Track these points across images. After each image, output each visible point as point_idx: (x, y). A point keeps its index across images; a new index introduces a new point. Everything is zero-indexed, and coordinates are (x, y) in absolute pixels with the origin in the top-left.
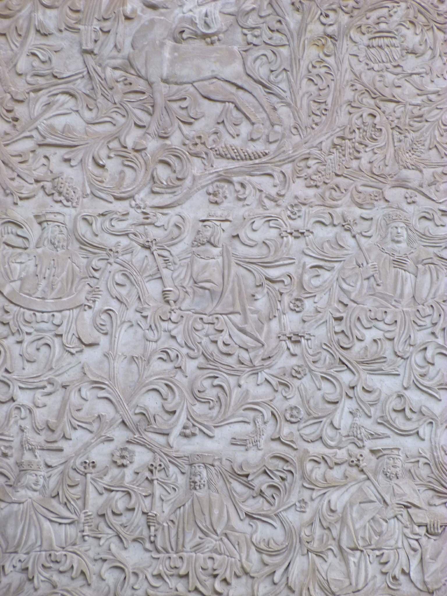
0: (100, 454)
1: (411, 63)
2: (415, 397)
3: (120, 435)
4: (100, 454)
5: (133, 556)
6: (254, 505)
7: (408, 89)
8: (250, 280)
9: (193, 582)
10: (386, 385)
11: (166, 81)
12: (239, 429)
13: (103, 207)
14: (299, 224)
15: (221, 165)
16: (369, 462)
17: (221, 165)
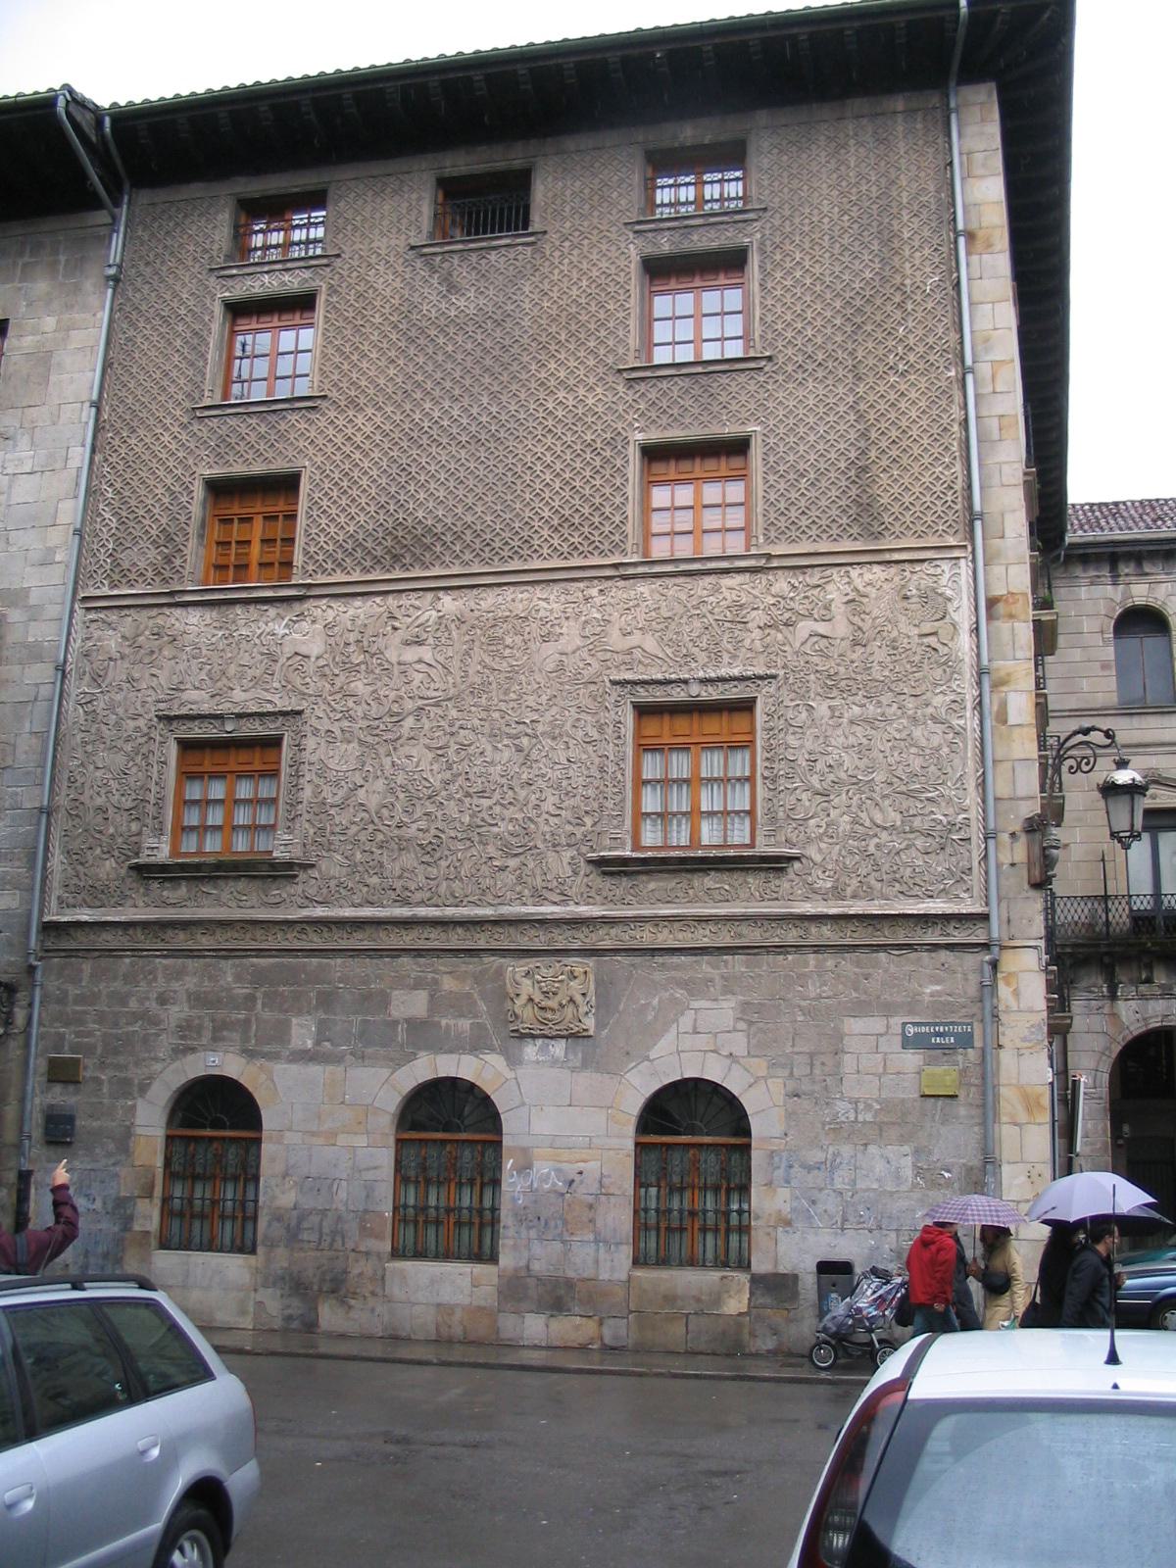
0: (363, 837)
1: (507, 652)
2: (497, 809)
3: (371, 827)
4: (363, 837)
5: (375, 880)
6: (427, 858)
7: (505, 664)
8: (430, 755)
9: (398, 892)
10: (486, 803)
11: (399, 664)
12: (422, 824)
13: (368, 723)
14: (454, 730)
15: (420, 702)
16: (476, 839)
17: (420, 702)
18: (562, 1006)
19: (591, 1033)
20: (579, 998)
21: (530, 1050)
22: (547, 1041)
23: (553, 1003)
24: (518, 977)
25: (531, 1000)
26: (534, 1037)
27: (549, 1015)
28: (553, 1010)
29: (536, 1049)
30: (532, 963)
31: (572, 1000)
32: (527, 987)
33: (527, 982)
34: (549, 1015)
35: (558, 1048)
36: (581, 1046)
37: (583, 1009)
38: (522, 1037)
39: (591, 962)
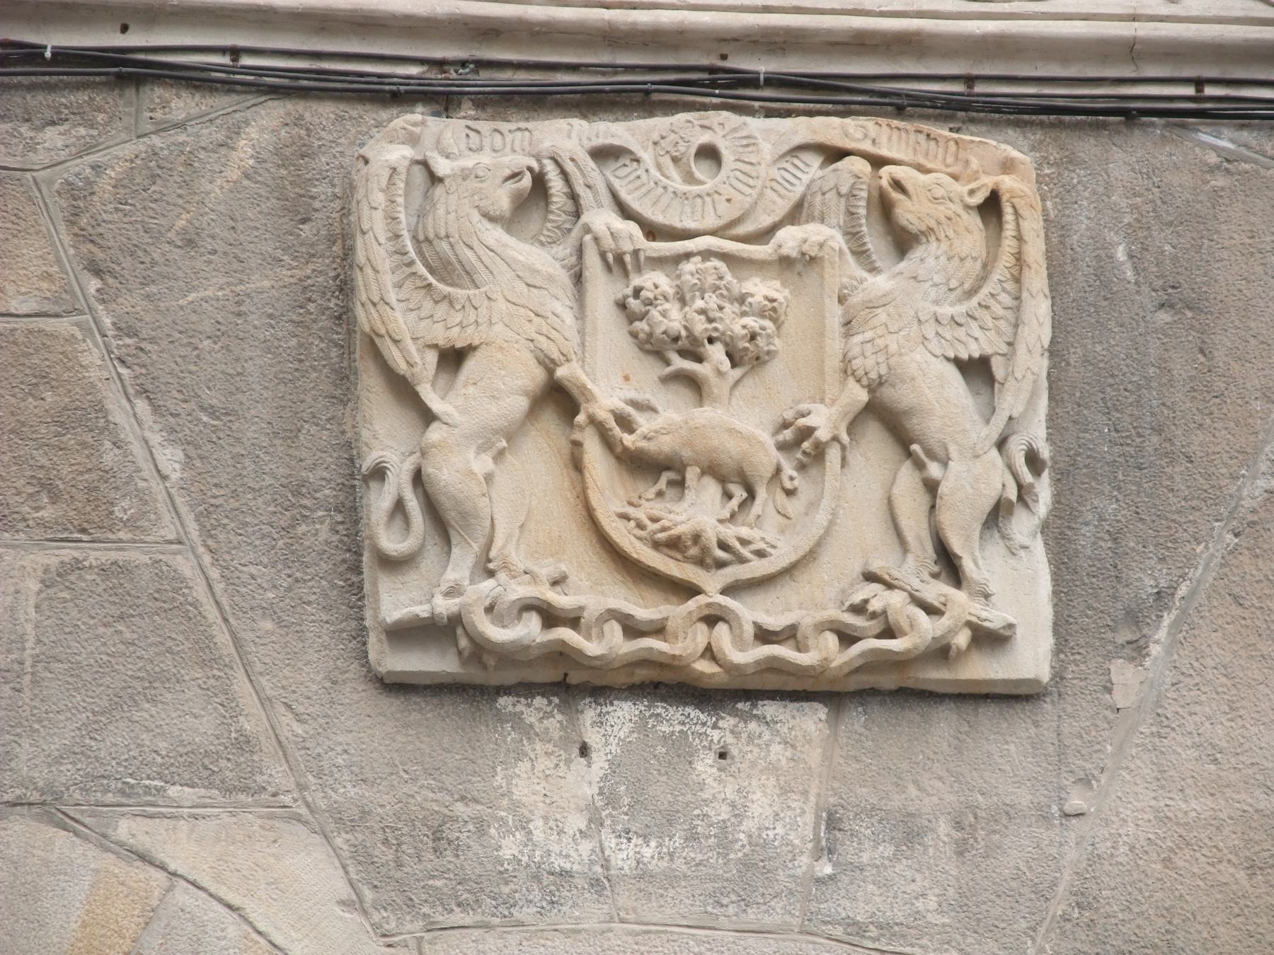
18: (801, 444)
19: (1031, 658)
20: (940, 398)
21: (550, 790)
22: (674, 719)
23: (740, 420)
24: (455, 213)
25: (558, 398)
26: (570, 682)
27: (700, 510)
28: (737, 481)
29: (584, 781)
30: (567, 136)
31: (886, 418)
32: (524, 305)
33: (534, 257)
34: (700, 510)
35: (768, 777)
36: (930, 765)
37: (974, 478)
38: (476, 681)
39: (1003, 159)
